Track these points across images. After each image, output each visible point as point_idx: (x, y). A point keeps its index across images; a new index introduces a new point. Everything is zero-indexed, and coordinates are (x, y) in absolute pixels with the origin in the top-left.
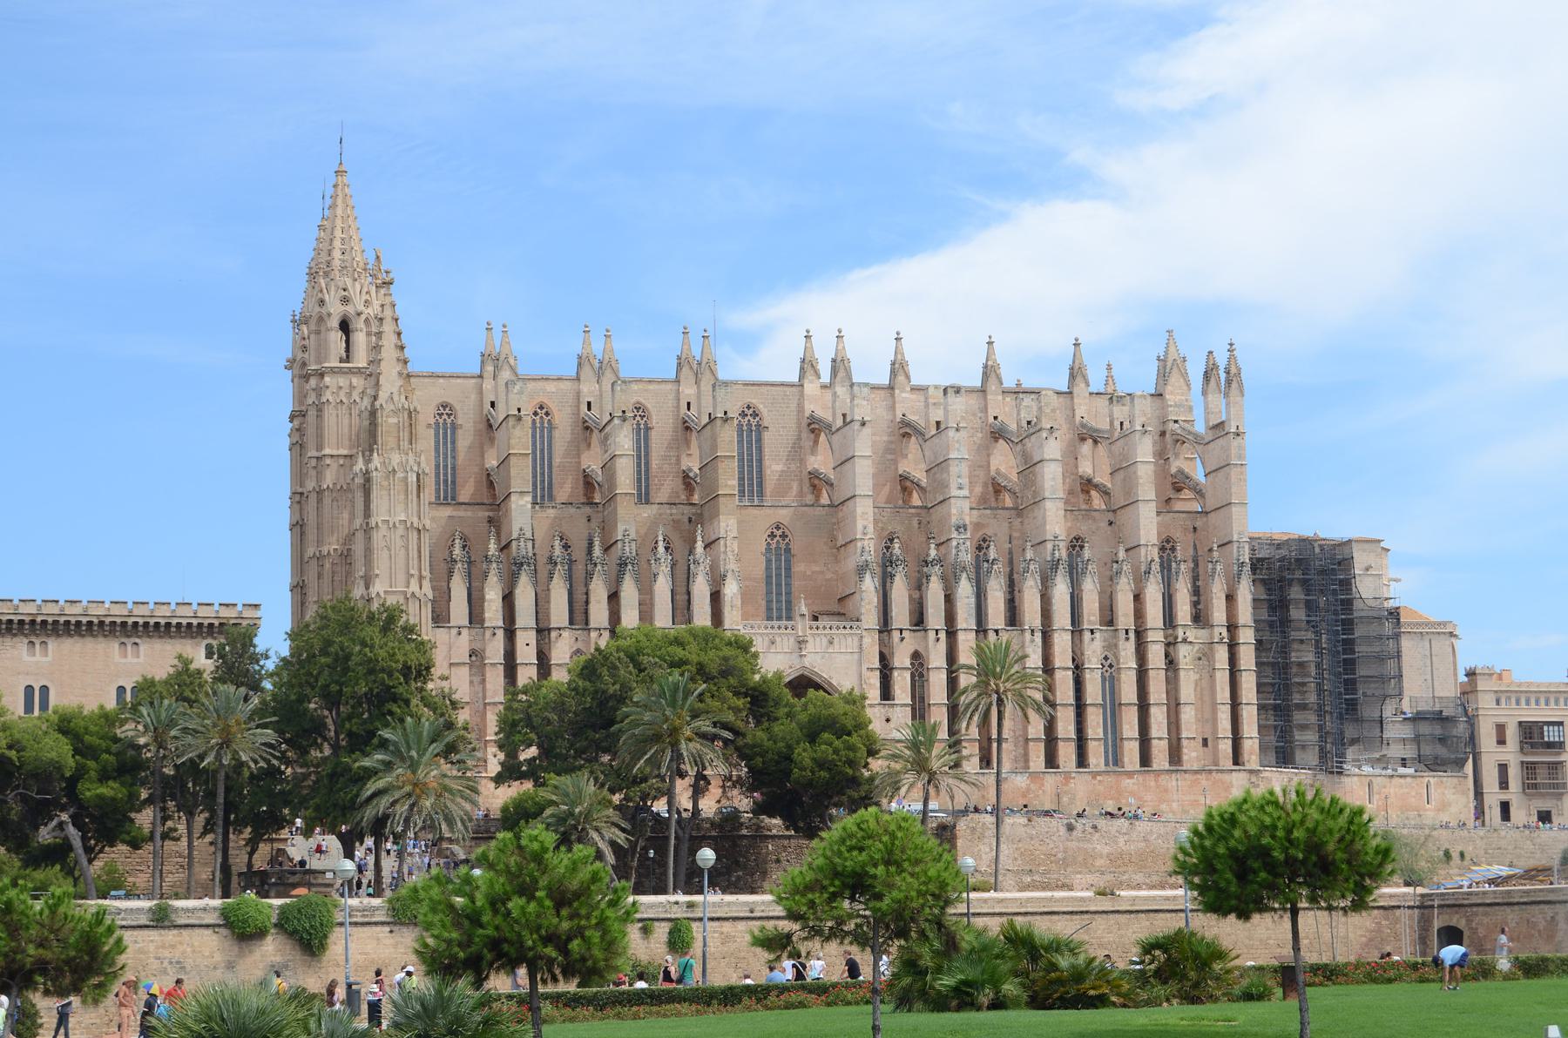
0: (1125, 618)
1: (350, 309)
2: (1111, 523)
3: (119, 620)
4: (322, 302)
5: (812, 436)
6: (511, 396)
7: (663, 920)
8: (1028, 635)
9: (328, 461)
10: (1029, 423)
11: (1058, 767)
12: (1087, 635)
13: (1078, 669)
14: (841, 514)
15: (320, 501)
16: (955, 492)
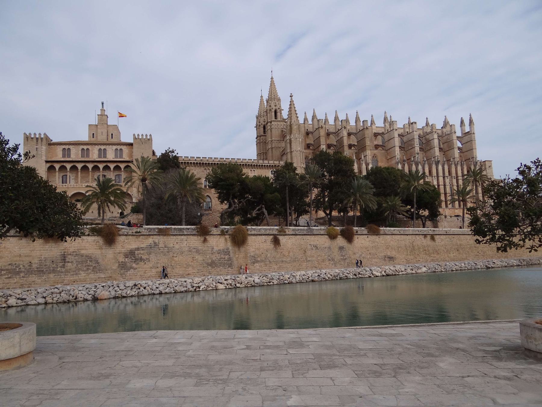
0: (454, 174)
1: (277, 108)
2: (444, 155)
3: (250, 164)
4: (270, 106)
5: (375, 137)
6: (320, 122)
7: (428, 235)
8: (434, 177)
9: (274, 141)
10: (426, 132)
11: (442, 207)
12: (446, 177)
13: (445, 185)
14: (388, 152)
15: (272, 150)
16: (416, 146)
